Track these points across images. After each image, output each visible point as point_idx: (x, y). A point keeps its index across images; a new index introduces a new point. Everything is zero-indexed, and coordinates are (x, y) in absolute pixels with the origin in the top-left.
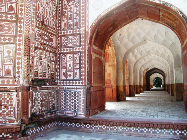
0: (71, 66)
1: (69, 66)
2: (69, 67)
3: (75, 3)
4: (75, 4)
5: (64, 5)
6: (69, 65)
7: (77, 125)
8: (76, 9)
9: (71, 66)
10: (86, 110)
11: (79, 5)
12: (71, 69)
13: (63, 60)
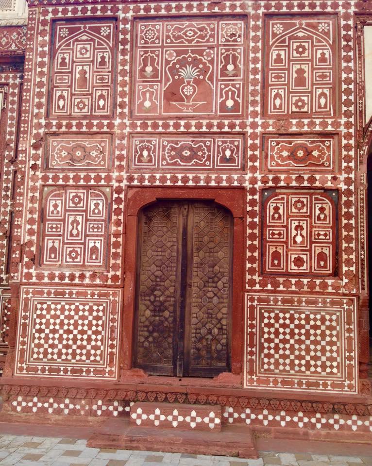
0: (304, 233)
1: (294, 232)
2: (295, 236)
3: (316, 34)
4: (315, 36)
5: (274, 35)
6: (296, 228)
7: (296, 419)
8: (319, 52)
9: (304, 233)
10: (360, 371)
11: (331, 42)
12: (302, 242)
13: (274, 214)
